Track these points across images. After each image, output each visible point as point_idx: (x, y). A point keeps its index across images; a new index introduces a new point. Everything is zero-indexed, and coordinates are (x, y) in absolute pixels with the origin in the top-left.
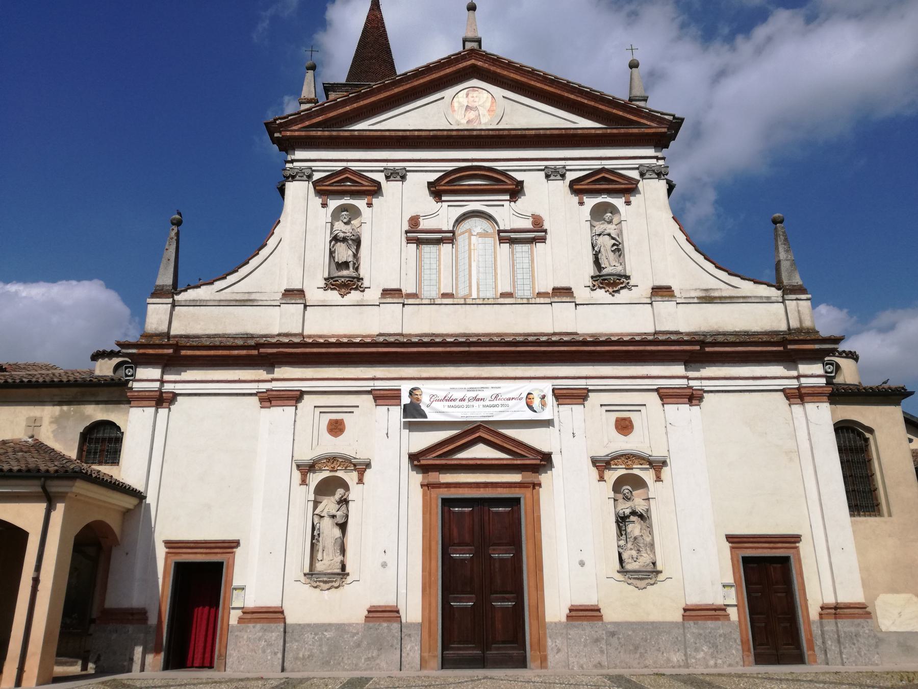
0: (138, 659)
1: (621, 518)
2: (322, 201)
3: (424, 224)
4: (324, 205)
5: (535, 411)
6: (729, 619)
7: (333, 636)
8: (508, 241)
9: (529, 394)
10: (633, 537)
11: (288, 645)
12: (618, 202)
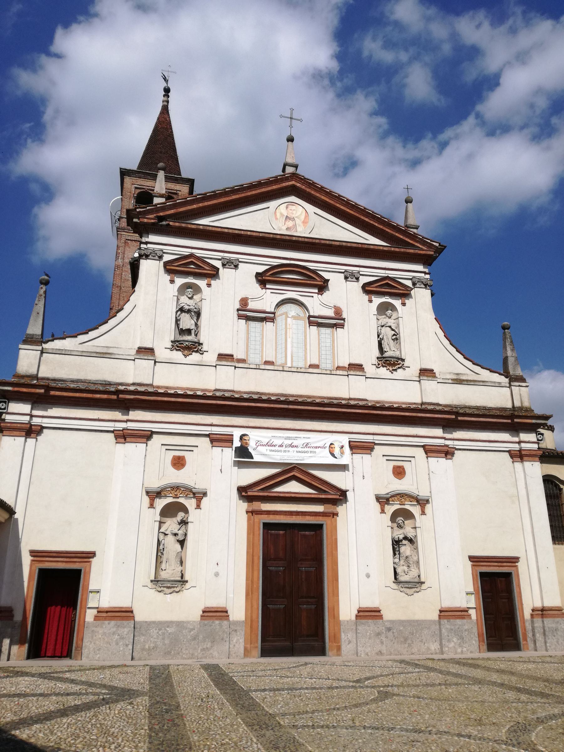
0: (6, 649)
1: (396, 541)
2: (171, 278)
3: (252, 305)
4: (172, 281)
5: (336, 458)
6: (471, 618)
7: (174, 631)
8: (316, 324)
9: (331, 444)
10: (405, 556)
11: (136, 638)
12: (397, 303)
